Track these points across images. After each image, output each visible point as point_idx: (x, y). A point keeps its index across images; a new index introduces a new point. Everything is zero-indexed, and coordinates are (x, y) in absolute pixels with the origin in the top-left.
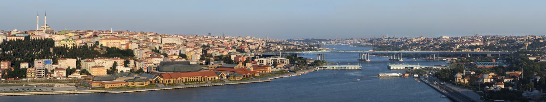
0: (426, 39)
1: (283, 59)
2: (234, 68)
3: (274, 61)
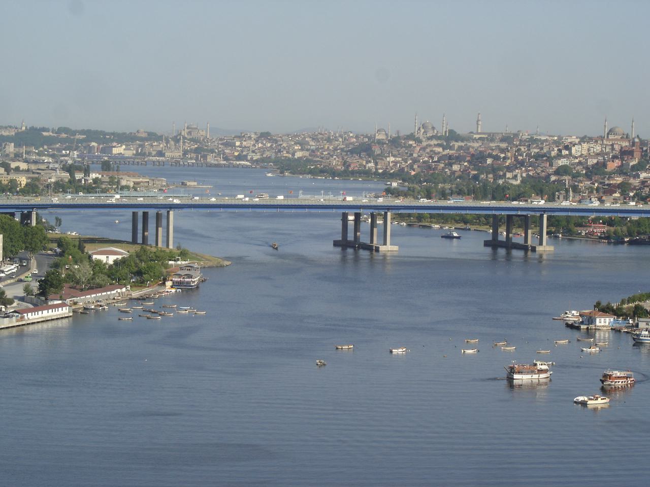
0: (634, 144)
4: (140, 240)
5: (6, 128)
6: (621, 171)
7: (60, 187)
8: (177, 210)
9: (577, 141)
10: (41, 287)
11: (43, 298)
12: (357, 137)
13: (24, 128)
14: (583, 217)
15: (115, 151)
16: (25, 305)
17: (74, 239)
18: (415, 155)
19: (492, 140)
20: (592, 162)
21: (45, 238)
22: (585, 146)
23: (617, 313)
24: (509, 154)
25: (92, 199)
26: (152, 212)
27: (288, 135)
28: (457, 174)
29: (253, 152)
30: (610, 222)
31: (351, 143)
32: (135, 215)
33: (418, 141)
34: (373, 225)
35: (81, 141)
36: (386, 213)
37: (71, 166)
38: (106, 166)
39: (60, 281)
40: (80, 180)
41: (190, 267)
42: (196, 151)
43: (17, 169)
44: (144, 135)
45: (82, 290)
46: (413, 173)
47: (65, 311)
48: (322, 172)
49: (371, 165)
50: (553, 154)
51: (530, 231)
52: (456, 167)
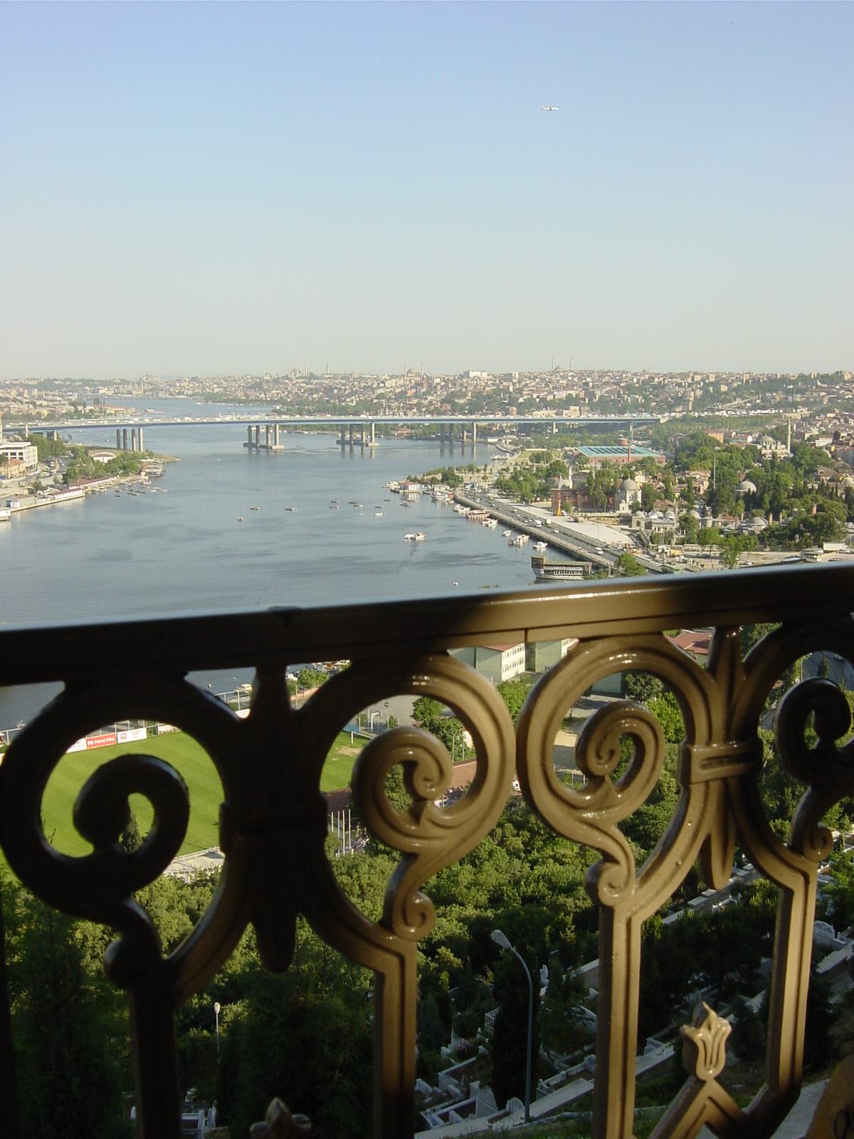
1: (21, 448)
4: (122, 447)
5: (31, 379)
6: (416, 395)
7: (69, 415)
9: (388, 378)
10: (64, 479)
12: (252, 378)
13: (43, 380)
14: (395, 425)
15: (101, 392)
16: (55, 490)
17: (81, 447)
18: (289, 389)
19: (336, 379)
20: (398, 390)
21: (63, 448)
22: (394, 380)
23: (421, 482)
24: (347, 387)
25: (90, 422)
26: (129, 430)
27: (209, 378)
28: (316, 400)
29: (188, 389)
30: (412, 427)
31: (250, 383)
33: (291, 380)
34: (267, 432)
35: (79, 386)
36: (275, 425)
37: (74, 402)
38: (97, 401)
39: (75, 473)
40: (81, 411)
41: (155, 463)
42: (152, 390)
43: (41, 405)
44: (119, 381)
45: (89, 479)
46: (289, 400)
47: (81, 493)
48: (232, 401)
49: (263, 395)
50: (374, 386)
51: (364, 433)
52: (315, 396)
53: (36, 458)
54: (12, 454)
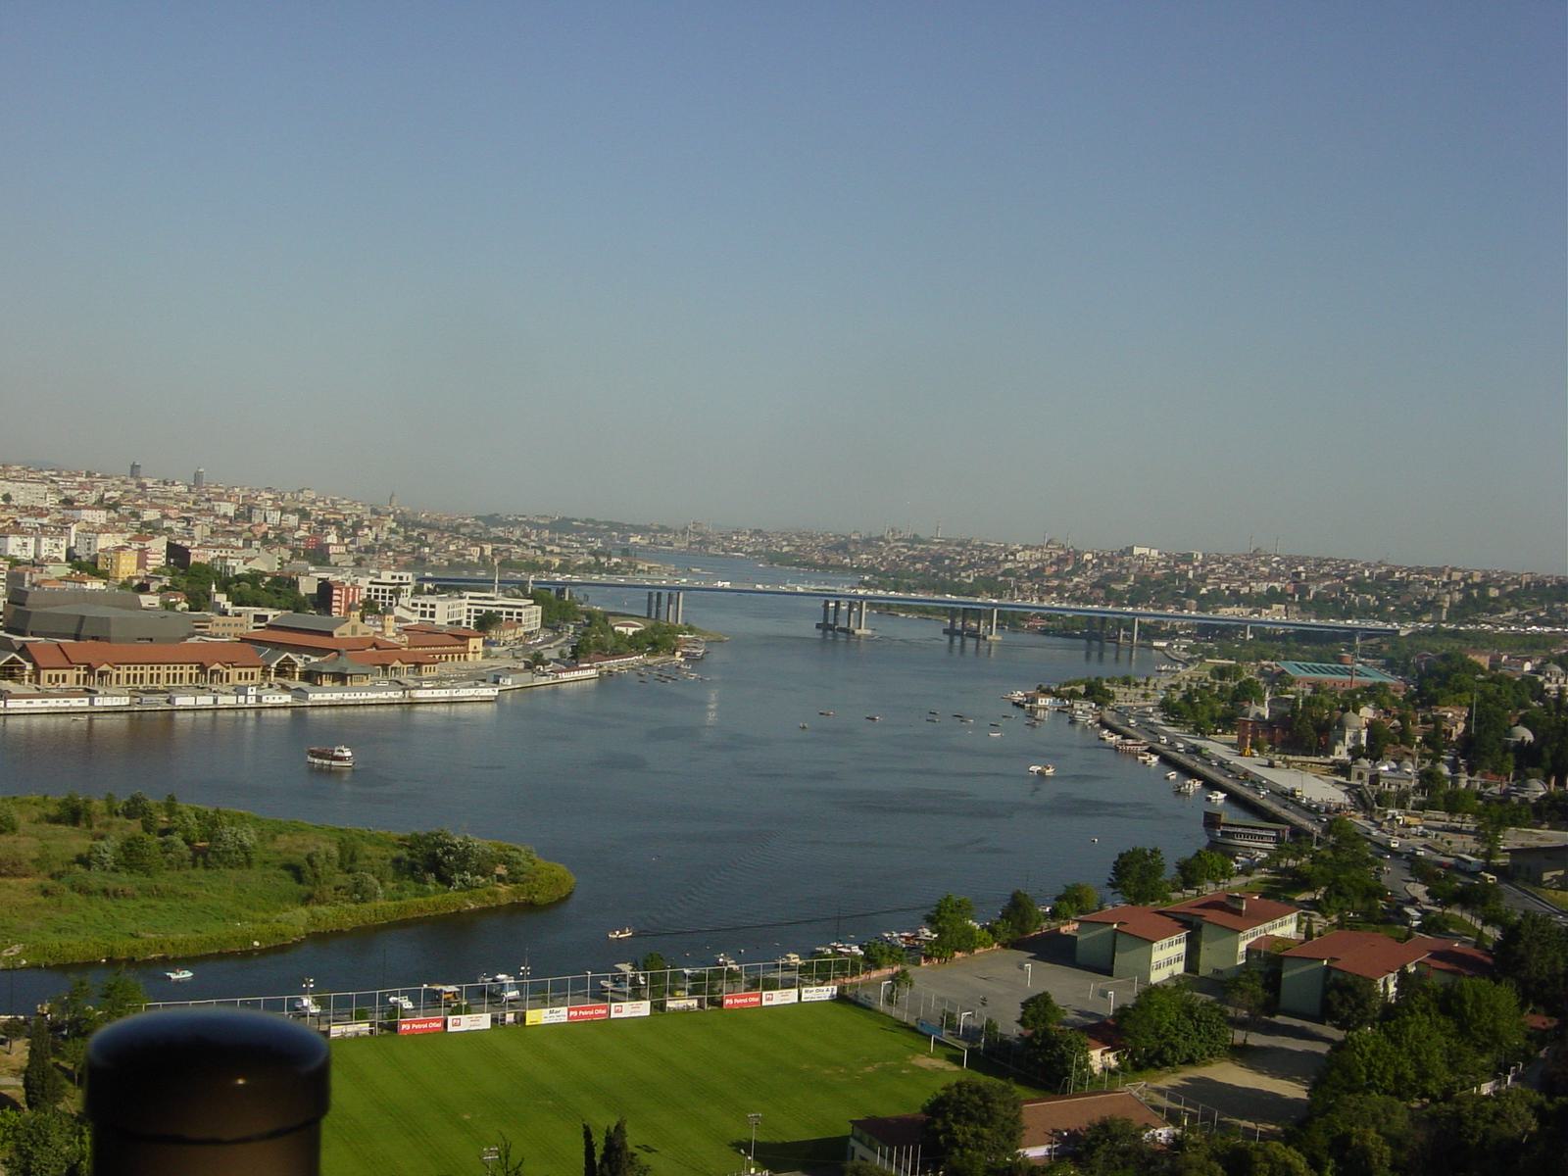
0: (1069, 553)
1: (520, 607)
2: (330, 634)
3: (476, 611)
6: (1057, 575)
7: (587, 568)
8: (686, 592)
9: (1020, 548)
11: (574, 661)
12: (835, 536)
14: (1026, 613)
15: (632, 540)
18: (884, 554)
19: (950, 545)
20: (1033, 566)
22: (1028, 552)
24: (964, 557)
26: (665, 594)
27: (777, 532)
28: (919, 572)
29: (747, 545)
30: (1049, 618)
31: (831, 542)
32: (650, 594)
33: (888, 542)
34: (850, 610)
36: (862, 603)
38: (625, 553)
39: (589, 647)
40: (604, 564)
41: (696, 641)
45: (606, 656)
46: (882, 569)
47: (592, 673)
49: (848, 560)
50: (1001, 558)
51: (982, 622)
52: (919, 566)
53: (539, 621)
54: (508, 613)
